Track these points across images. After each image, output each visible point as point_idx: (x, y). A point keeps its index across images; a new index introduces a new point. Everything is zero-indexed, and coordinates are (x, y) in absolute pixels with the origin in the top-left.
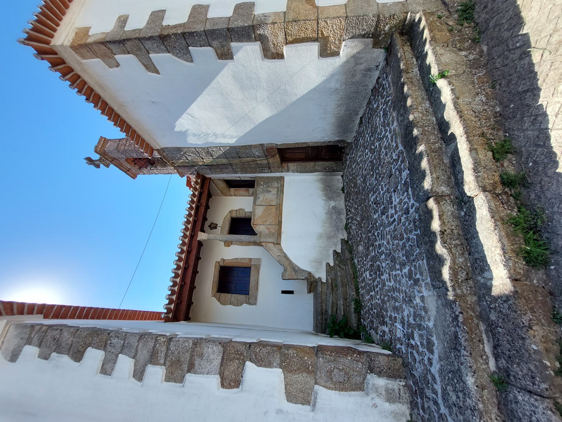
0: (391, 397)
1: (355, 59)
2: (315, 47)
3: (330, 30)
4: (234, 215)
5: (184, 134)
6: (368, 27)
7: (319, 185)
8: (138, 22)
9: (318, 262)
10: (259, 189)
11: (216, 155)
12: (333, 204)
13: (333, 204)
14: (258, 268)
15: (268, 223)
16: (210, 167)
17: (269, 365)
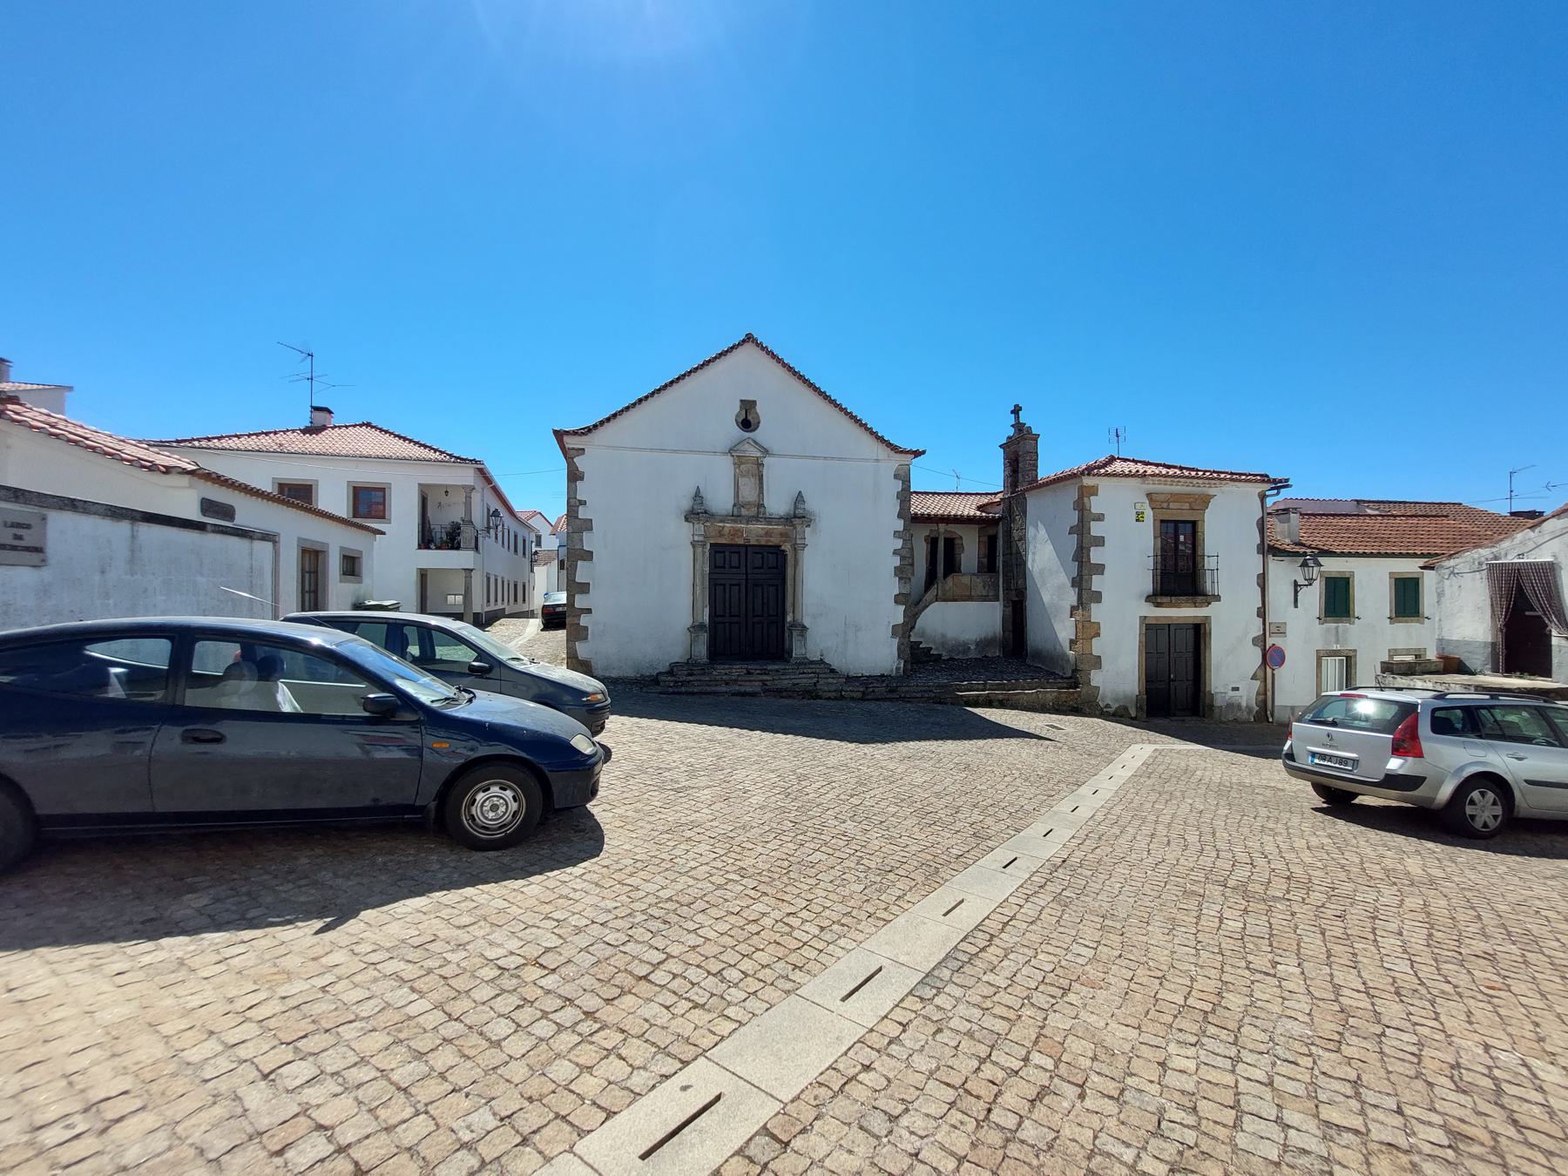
1: (1064, 657)
3: (1079, 645)
5: (1036, 527)
7: (990, 635)
8: (1096, 529)
9: (923, 634)
10: (986, 577)
16: (1008, 533)
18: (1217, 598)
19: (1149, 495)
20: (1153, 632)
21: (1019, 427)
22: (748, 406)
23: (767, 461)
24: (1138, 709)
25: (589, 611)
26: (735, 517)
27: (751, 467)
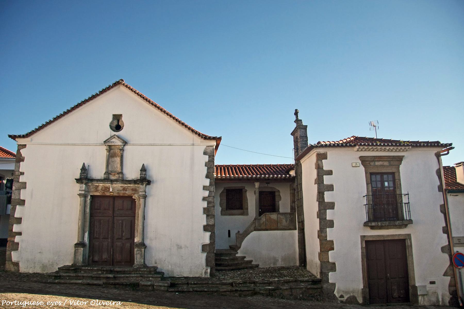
0: (206, 273)
4: (277, 194)
8: (327, 180)
12: (280, 260)
13: (280, 260)
14: (242, 214)
15: (267, 223)
17: (210, 239)
18: (410, 221)
19: (361, 158)
20: (369, 245)
21: (298, 121)
22: (117, 118)
23: (126, 147)
24: (364, 298)
25: (20, 234)
26: (106, 180)
27: (114, 152)
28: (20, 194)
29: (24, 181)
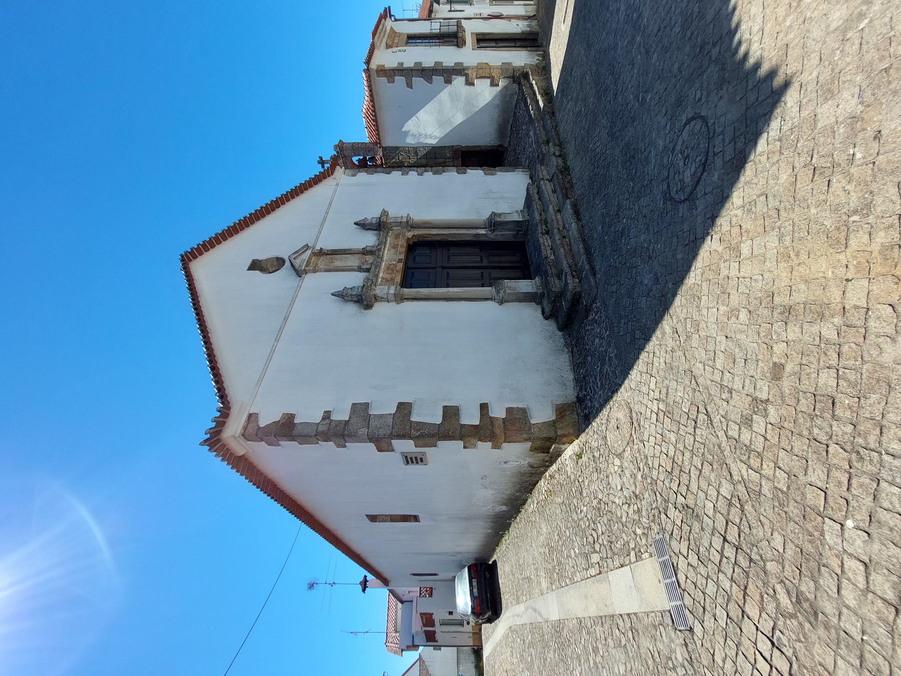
2: (489, 81)
3: (495, 74)
6: (510, 74)
11: (420, 154)
19: (388, 46)
22: (255, 266)
25: (484, 407)
28: (381, 416)
29: (349, 407)
